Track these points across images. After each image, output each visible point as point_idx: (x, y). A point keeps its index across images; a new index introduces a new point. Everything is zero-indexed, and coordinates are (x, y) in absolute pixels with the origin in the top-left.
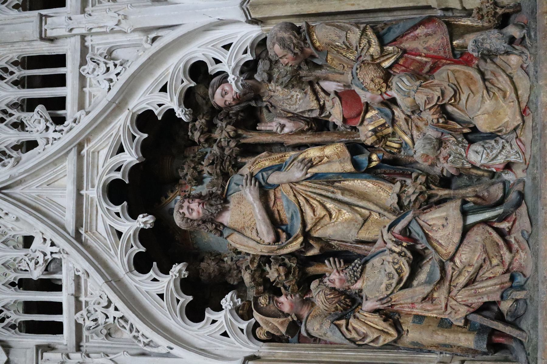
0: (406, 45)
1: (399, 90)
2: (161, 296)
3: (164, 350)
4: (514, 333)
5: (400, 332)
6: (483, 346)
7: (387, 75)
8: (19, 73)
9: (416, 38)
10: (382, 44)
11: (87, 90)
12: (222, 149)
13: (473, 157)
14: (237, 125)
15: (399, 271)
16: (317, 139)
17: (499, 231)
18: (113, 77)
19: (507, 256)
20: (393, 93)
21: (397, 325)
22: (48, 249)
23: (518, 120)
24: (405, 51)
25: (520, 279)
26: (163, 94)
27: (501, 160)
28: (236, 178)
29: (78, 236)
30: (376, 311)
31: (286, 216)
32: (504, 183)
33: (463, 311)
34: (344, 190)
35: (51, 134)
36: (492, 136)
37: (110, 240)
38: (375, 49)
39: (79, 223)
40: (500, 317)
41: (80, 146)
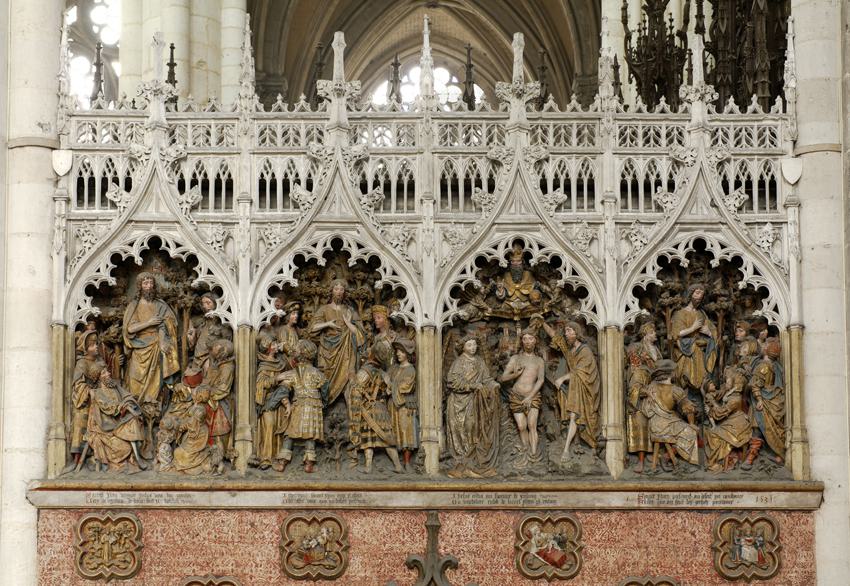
0: (218, 412)
1: (196, 409)
2: (98, 271)
3: (68, 278)
4: (79, 466)
5: (79, 408)
6: (73, 451)
7: (204, 403)
8: (224, 178)
9: (222, 417)
10: (219, 401)
11: (210, 225)
12: (182, 298)
13: (162, 446)
14: (193, 308)
15: (108, 409)
16: (184, 353)
17: (128, 457)
18: (214, 245)
19: (116, 461)
20: (195, 405)
21: (83, 407)
22: (122, 204)
23: (179, 468)
24: (216, 412)
25: (105, 468)
26: (206, 271)
27: (161, 460)
28: (165, 306)
29: (130, 221)
30: (89, 395)
31: (142, 338)
32: (153, 459)
33: (90, 440)
34: (155, 371)
35: (185, 206)
36: (173, 454)
37: (129, 240)
38: (217, 397)
39: (137, 222)
40: (88, 456)
41: (178, 222)
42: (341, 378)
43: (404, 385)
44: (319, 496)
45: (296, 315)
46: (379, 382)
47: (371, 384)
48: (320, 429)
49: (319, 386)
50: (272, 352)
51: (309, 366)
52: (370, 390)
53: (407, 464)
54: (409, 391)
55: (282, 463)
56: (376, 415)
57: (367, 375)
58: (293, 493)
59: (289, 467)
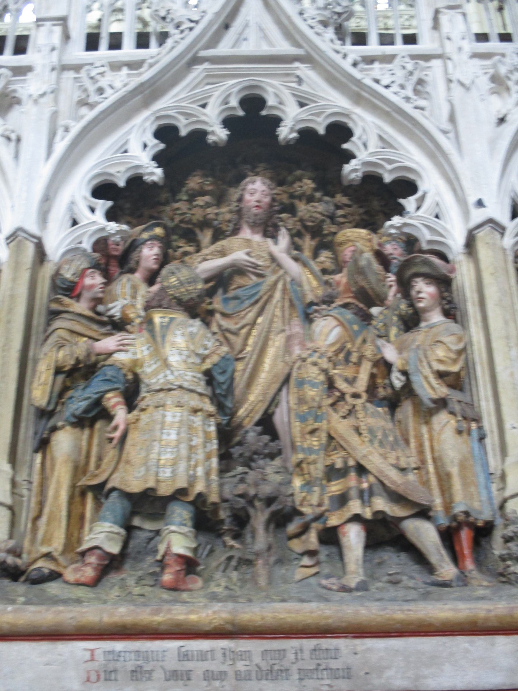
42: (263, 377)
43: (440, 352)
44: (203, 656)
45: (156, 250)
46: (369, 351)
47: (349, 354)
48: (208, 474)
49: (207, 365)
50: (87, 295)
51: (180, 317)
52: (349, 372)
53: (469, 565)
54: (455, 368)
55: (92, 559)
56: (371, 431)
57: (338, 331)
58: (119, 646)
59: (114, 578)
